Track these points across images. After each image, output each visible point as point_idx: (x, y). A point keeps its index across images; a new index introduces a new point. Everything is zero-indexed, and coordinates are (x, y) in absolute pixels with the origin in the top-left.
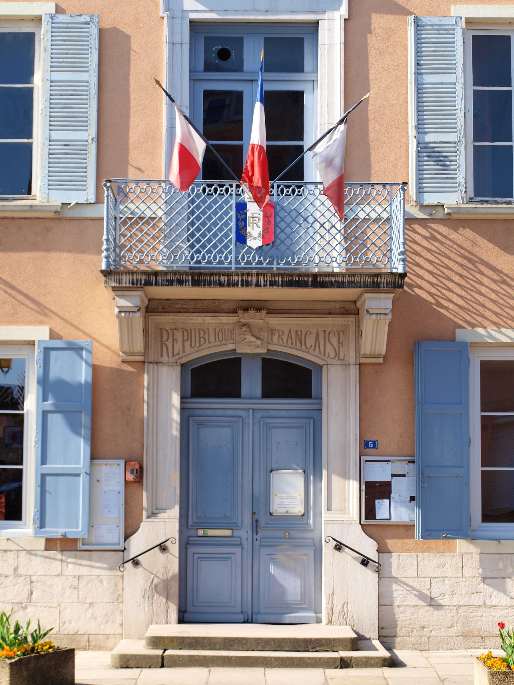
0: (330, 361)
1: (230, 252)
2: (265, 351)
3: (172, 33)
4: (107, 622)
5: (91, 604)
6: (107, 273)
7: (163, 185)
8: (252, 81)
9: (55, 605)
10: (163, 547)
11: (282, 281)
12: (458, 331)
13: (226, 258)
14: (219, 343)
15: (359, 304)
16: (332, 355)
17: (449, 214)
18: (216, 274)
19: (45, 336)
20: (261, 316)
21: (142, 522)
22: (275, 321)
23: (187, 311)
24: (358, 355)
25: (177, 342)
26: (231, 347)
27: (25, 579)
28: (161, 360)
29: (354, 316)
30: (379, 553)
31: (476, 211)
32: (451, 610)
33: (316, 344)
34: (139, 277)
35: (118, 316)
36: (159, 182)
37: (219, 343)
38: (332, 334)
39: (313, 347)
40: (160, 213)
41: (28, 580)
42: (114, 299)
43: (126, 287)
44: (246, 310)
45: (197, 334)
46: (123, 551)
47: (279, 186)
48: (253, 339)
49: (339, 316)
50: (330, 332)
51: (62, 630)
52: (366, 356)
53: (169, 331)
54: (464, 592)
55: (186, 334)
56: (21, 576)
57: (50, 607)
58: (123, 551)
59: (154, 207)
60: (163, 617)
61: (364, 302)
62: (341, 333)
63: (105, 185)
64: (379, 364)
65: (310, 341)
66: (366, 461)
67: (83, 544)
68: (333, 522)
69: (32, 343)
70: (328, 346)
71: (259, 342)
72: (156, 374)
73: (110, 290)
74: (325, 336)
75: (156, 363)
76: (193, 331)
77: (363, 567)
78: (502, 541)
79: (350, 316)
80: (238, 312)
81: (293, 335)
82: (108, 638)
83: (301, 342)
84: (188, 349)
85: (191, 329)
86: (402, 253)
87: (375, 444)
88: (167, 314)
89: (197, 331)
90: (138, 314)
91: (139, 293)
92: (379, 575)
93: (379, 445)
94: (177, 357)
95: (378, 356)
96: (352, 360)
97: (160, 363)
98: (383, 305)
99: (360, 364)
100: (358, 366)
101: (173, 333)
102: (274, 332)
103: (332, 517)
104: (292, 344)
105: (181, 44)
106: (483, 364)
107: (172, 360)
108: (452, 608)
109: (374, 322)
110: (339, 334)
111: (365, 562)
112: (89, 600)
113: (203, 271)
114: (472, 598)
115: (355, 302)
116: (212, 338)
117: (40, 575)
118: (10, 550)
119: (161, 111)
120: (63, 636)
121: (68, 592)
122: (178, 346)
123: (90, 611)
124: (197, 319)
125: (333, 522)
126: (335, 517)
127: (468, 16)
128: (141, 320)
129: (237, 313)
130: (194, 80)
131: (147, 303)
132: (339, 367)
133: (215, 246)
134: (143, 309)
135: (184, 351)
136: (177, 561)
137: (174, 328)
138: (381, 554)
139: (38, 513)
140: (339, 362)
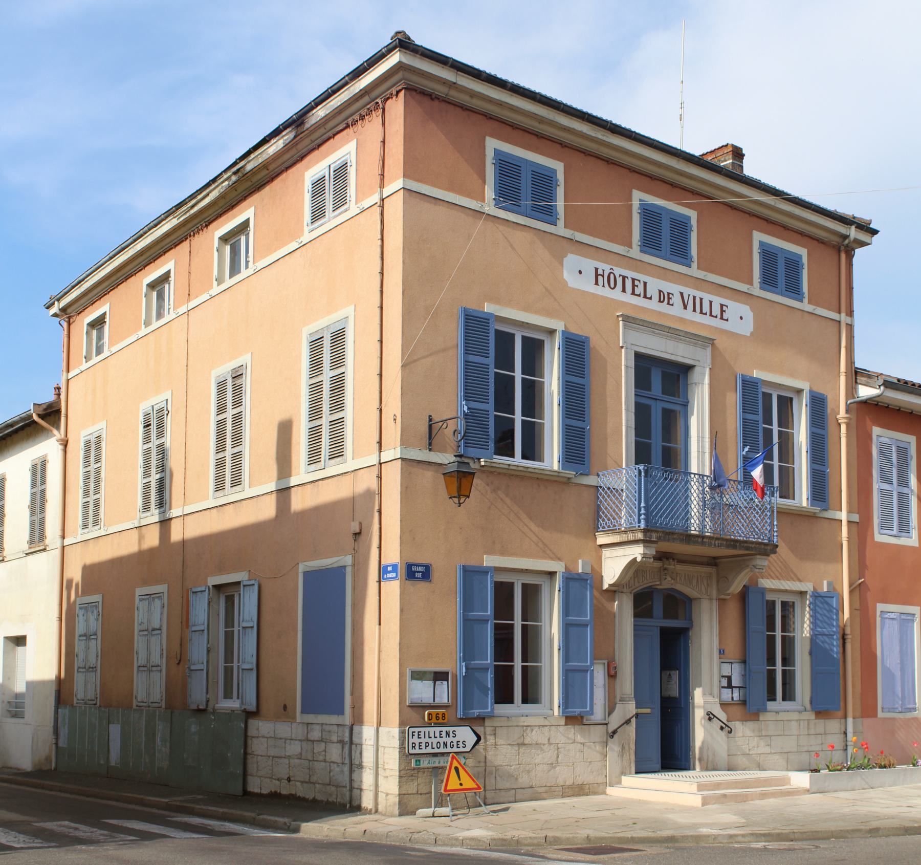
5: (590, 762)
7: (696, 476)
8: (656, 399)
9: (571, 764)
10: (628, 722)
12: (759, 580)
16: (704, 592)
21: (616, 704)
22: (680, 568)
44: (667, 559)
48: (670, 579)
60: (628, 769)
67: (587, 720)
70: (703, 586)
82: (599, 786)
84: (637, 584)
87: (723, 651)
93: (725, 652)
96: (715, 597)
112: (589, 760)
116: (648, 577)
118: (546, 726)
136: (634, 730)
140: (708, 597)
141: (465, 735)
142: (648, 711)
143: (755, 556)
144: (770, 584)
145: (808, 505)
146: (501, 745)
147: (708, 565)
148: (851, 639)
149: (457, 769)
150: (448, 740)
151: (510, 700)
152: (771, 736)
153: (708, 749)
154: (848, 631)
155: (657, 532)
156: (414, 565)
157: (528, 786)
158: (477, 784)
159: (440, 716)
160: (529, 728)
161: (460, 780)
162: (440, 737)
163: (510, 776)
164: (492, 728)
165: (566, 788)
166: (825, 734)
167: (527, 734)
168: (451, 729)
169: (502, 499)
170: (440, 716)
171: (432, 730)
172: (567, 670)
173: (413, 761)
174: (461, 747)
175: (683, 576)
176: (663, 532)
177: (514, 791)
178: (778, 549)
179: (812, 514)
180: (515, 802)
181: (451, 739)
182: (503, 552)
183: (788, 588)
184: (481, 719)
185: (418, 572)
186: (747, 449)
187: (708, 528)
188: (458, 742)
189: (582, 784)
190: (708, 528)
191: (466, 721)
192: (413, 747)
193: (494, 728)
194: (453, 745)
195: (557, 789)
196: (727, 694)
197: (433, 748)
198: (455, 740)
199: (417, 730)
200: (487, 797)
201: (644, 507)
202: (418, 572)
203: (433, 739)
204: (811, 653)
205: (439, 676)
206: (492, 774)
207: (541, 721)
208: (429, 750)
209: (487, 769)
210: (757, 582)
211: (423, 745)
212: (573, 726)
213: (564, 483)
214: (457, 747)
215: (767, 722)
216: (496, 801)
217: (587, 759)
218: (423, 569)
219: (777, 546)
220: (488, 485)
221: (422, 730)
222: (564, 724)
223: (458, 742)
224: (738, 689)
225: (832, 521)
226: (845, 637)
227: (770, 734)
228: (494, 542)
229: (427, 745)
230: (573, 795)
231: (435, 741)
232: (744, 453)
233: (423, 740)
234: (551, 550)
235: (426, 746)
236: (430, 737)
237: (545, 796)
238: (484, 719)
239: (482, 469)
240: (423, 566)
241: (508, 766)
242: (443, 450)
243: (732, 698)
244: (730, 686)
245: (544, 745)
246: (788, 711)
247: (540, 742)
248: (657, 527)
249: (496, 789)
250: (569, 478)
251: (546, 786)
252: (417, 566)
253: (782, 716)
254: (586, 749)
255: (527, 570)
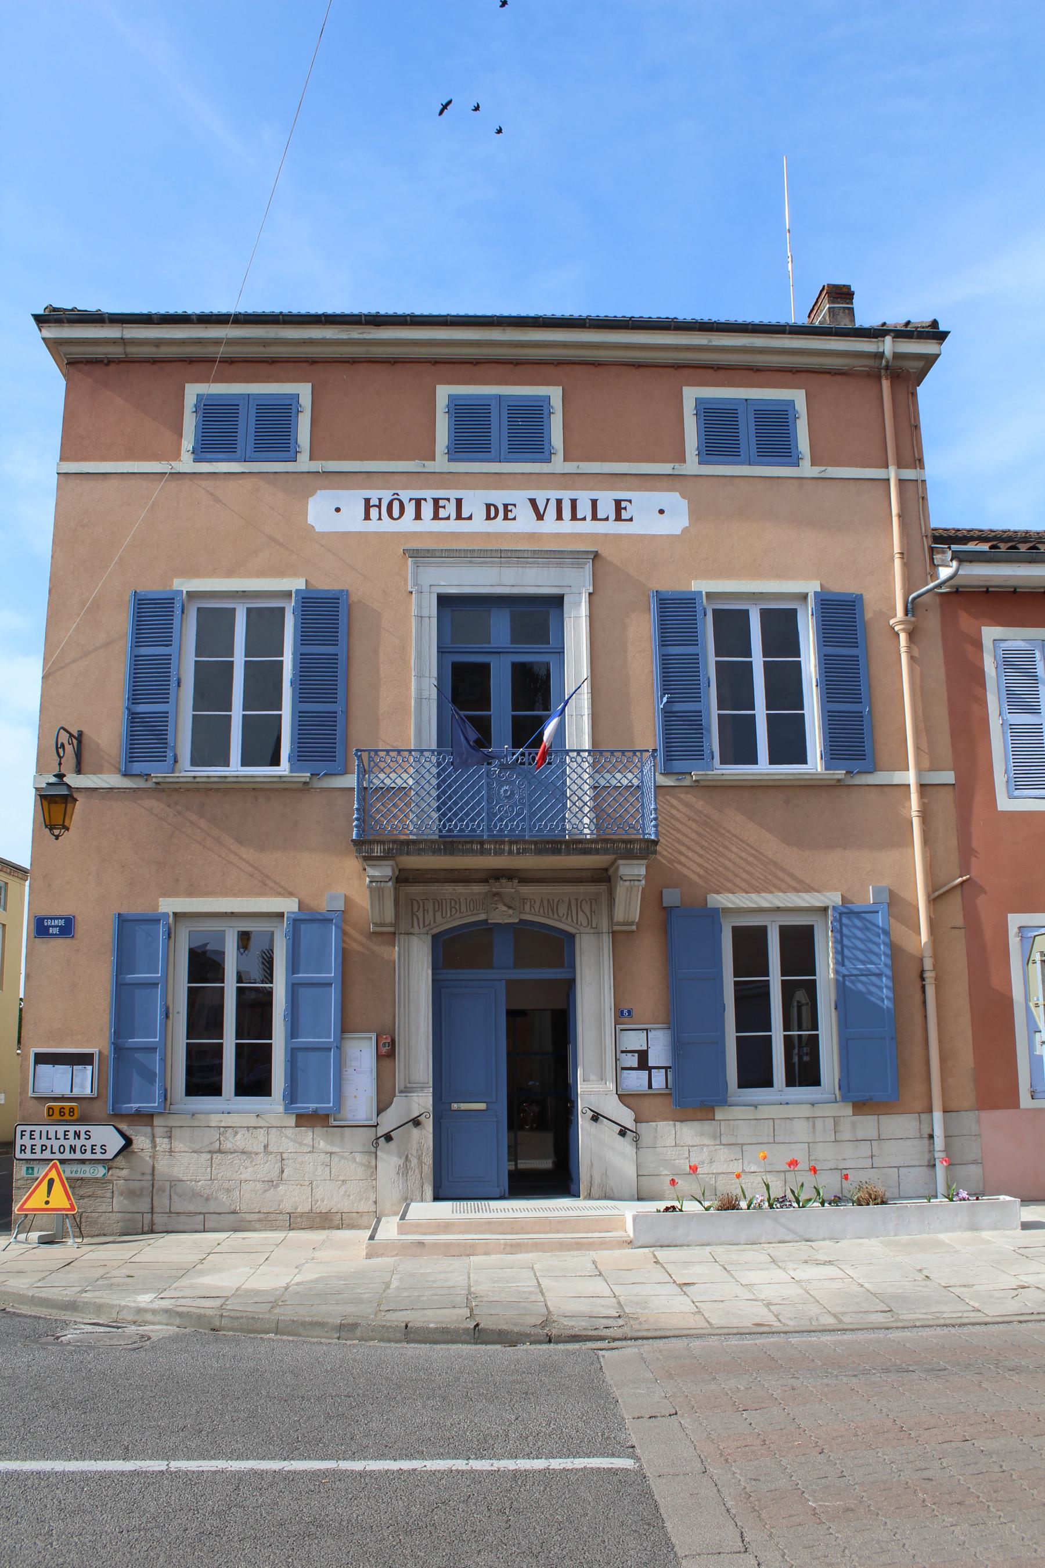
0: (582, 930)
1: (482, 820)
2: (517, 921)
3: (420, 607)
4: (361, 1200)
5: (343, 1181)
6: (358, 843)
9: (307, 1183)
10: (416, 1122)
11: (535, 848)
12: (708, 896)
13: (479, 826)
14: (470, 913)
15: (611, 872)
16: (585, 923)
17: (696, 781)
18: (467, 842)
19: (295, 908)
20: (512, 885)
21: (395, 1096)
22: (526, 890)
23: (437, 881)
24: (610, 922)
25: (428, 912)
26: (482, 917)
27: (276, 1157)
28: (412, 930)
29: (605, 884)
30: (636, 1123)
31: (724, 777)
32: (710, 1178)
33: (568, 913)
34: (391, 846)
35: (369, 887)
36: (410, 751)
37: (470, 913)
38: (584, 903)
39: (565, 915)
40: (411, 782)
41: (279, 1157)
42: (365, 869)
43: (377, 856)
44: (497, 878)
45: (448, 905)
46: (375, 1126)
47: (530, 754)
48: (505, 908)
49: (590, 884)
50: (582, 901)
51: (314, 1208)
52: (619, 924)
53: (420, 901)
54: (722, 1160)
55: (436, 904)
56: (271, 1153)
57: (301, 1185)
58: (375, 1126)
59: (405, 776)
60: (418, 1193)
61: (618, 868)
62: (593, 901)
63: (356, 755)
64: (632, 932)
65: (563, 910)
66: (621, 1030)
68: (590, 1093)
69: (281, 915)
70: (580, 914)
71: (510, 911)
72: (407, 945)
73: (361, 860)
74: (577, 905)
75: (407, 934)
76: (444, 901)
77: (620, 1137)
78: (759, 1107)
79: (603, 884)
80: (490, 881)
81: (546, 903)
82: (361, 1216)
83: (553, 910)
84: (439, 919)
85: (442, 900)
86: (655, 819)
87: (629, 1012)
88: (418, 884)
89: (448, 901)
90: (390, 884)
91: (391, 862)
92: (637, 1144)
93: (634, 1014)
94: (428, 928)
95: (631, 924)
96: (605, 929)
97: (411, 934)
98: (636, 872)
99: (613, 932)
100: (611, 934)
101: (424, 903)
102: (526, 901)
103: (587, 1088)
104: (544, 913)
105: (429, 617)
106: (736, 930)
107: (423, 930)
108: (711, 1176)
109: (627, 890)
110: (591, 902)
111: (623, 1133)
112: (341, 1178)
113: (455, 839)
114: (731, 1166)
115: (606, 870)
116: (463, 909)
117: (291, 1153)
118: (260, 1127)
119: (410, 682)
120: (316, 1215)
121: (319, 1170)
122: (430, 917)
123: (343, 1189)
124: (449, 889)
125: (590, 1093)
126: (592, 1088)
127: (707, 591)
128: (392, 890)
129: (488, 882)
130: (442, 652)
131: (397, 873)
132: (592, 935)
133: (467, 814)
134: (394, 879)
135: (435, 922)
137: (424, 898)
138: (638, 1124)
139: (289, 1089)
140: (592, 931)
141: (106, 1137)
142: (482, 1106)
143: (616, 864)
144: (822, 898)
145: (822, 770)
146: (180, 1152)
147: (593, 882)
148: (937, 979)
149: (51, 1182)
150: (78, 1143)
151: (216, 1090)
152: (743, 1145)
153: (592, 1165)
154: (928, 964)
155: (378, 842)
156: (48, 919)
157: (227, 1211)
158: (72, 1204)
159: (67, 1112)
160: (230, 1131)
161: (48, 1197)
162: (65, 1139)
163: (195, 1195)
164: (166, 1129)
165: (296, 1217)
166: (879, 1139)
167: (227, 1139)
168: (82, 1129)
169: (192, 823)
170: (67, 1112)
171: (52, 1129)
172: (293, 1050)
173: (24, 1169)
174: (98, 1153)
175: (538, 902)
176: (394, 842)
177: (202, 1216)
178: (658, 848)
179: (833, 783)
180: (204, 1232)
181: (82, 1141)
182: (191, 892)
183: (781, 905)
184: (146, 1118)
185: (53, 927)
186: (665, 700)
187: (411, 827)
188: (92, 1146)
189: (329, 1212)
190: (411, 827)
191: (116, 1117)
192: (21, 1150)
193: (169, 1129)
194: (85, 1150)
195: (281, 1217)
196: (636, 1081)
197: (52, 1153)
198: (88, 1144)
199: (28, 1128)
200: (155, 1222)
201: (357, 809)
202: (53, 927)
203: (53, 1141)
204: (836, 1009)
205: (85, 1059)
206: (164, 1191)
207: (253, 1121)
208: (78, 1155)
209: (155, 1182)
210: (706, 900)
211: (38, 1149)
212: (311, 1129)
213: (301, 790)
214: (92, 1153)
215: (732, 1122)
216: (170, 1229)
217: (338, 1176)
218: (62, 923)
219: (655, 843)
220: (169, 806)
221: (37, 1128)
222: (293, 1124)
223: (92, 1146)
224: (663, 1071)
225: (886, 789)
226: (925, 976)
227: (740, 1141)
228: (177, 880)
229: (44, 1148)
230: (311, 1228)
231: (56, 1144)
232: (662, 706)
233: (38, 1143)
234: (275, 883)
235: (42, 1150)
236: (48, 1139)
237: (257, 1226)
238: (151, 1116)
239: (159, 787)
240: (62, 919)
241: (191, 1181)
242: (98, 770)
243: (650, 1086)
244: (643, 1063)
245: (257, 1154)
246: (787, 1103)
247: (250, 1149)
248: (494, 836)
249: (170, 1212)
250: (305, 783)
251: (258, 1213)
252: (51, 919)
253: (765, 1112)
254: (335, 1159)
255: (232, 913)
